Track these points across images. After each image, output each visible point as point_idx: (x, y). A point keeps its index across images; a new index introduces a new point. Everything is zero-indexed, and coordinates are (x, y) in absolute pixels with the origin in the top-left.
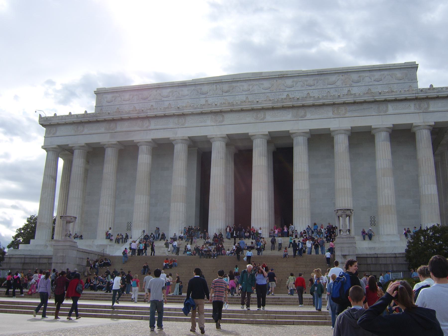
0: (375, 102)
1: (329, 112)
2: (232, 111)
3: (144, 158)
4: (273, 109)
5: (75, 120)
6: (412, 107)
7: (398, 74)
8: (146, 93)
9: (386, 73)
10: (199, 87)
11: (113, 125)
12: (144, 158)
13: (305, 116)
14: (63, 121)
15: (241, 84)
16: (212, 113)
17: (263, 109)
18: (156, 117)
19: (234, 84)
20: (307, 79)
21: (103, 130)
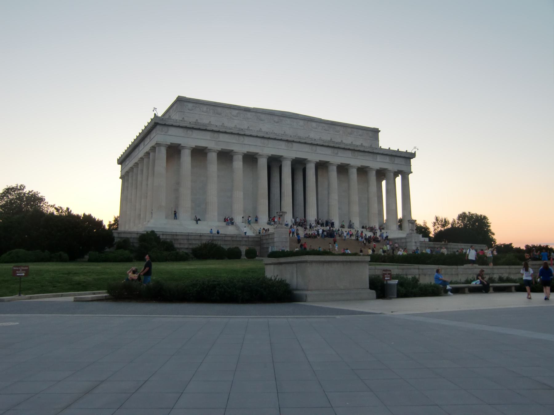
0: (373, 153)
1: (349, 153)
2: (299, 142)
3: (238, 164)
4: (322, 146)
5: (188, 125)
6: (387, 159)
7: (371, 134)
8: (219, 109)
9: (365, 131)
10: (259, 114)
11: (216, 135)
12: (238, 164)
13: (337, 154)
14: (178, 124)
15: (287, 119)
16: (287, 141)
17: (317, 145)
18: (251, 136)
19: (281, 118)
20: (324, 125)
21: (209, 138)
